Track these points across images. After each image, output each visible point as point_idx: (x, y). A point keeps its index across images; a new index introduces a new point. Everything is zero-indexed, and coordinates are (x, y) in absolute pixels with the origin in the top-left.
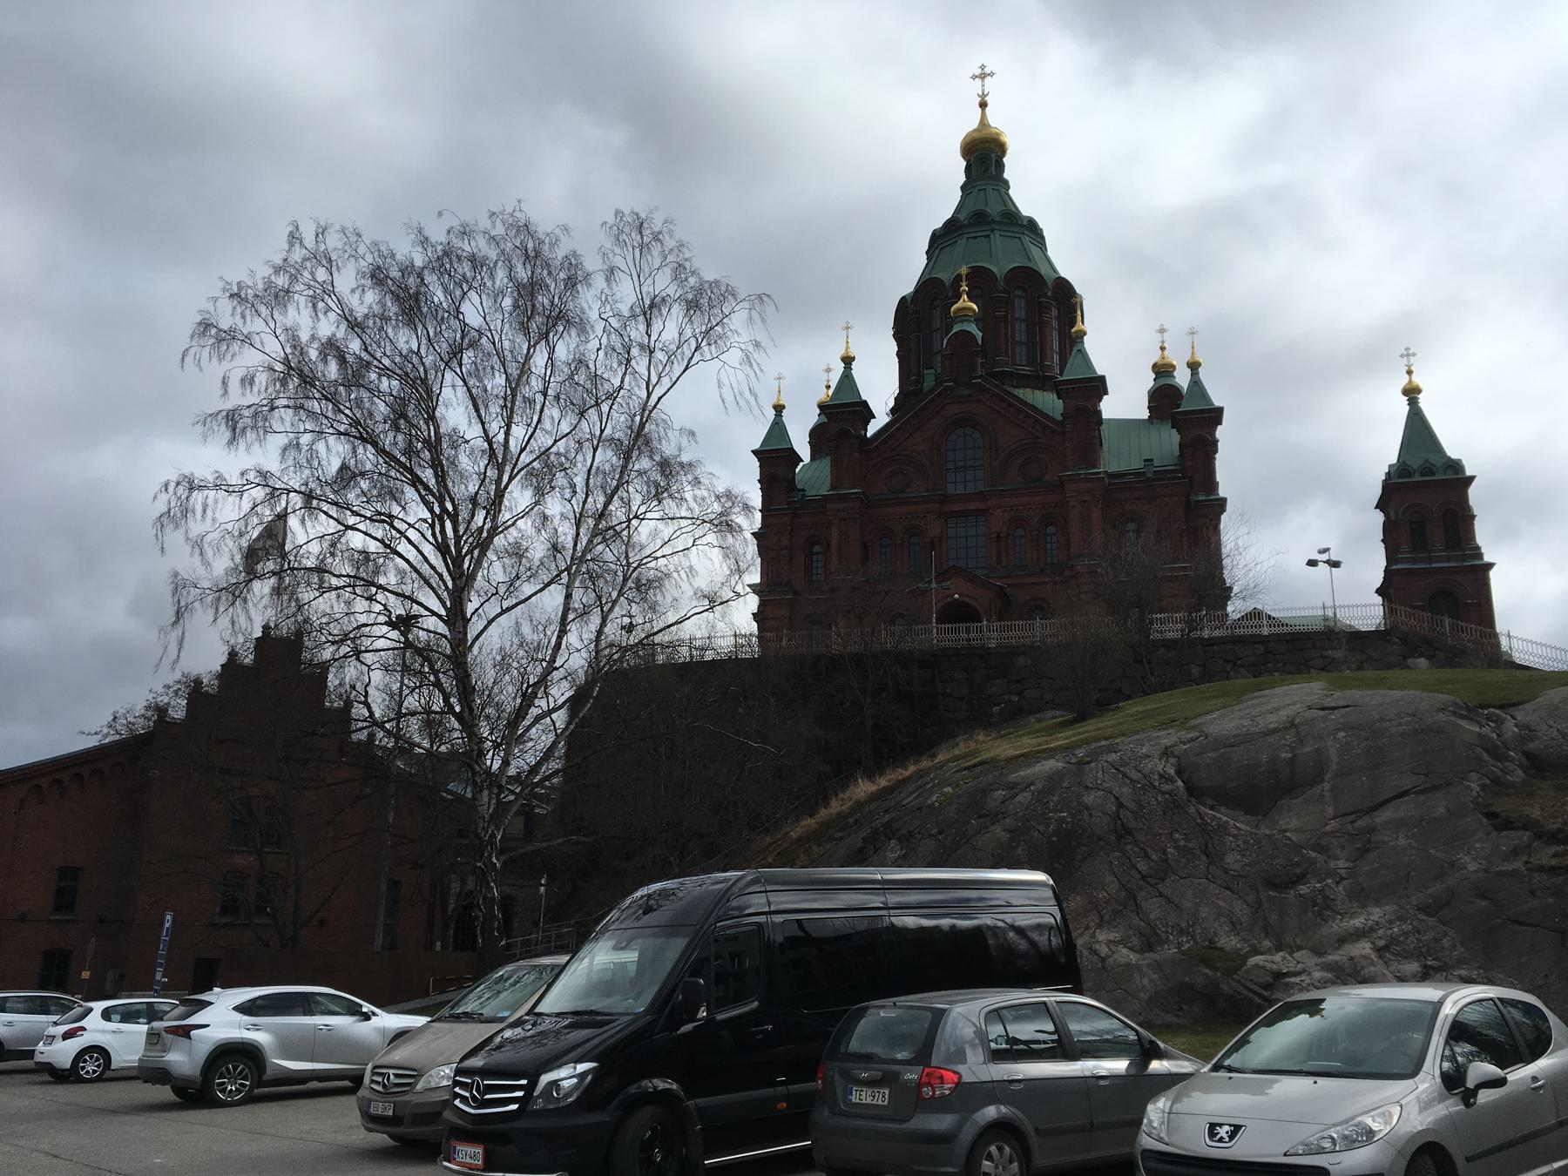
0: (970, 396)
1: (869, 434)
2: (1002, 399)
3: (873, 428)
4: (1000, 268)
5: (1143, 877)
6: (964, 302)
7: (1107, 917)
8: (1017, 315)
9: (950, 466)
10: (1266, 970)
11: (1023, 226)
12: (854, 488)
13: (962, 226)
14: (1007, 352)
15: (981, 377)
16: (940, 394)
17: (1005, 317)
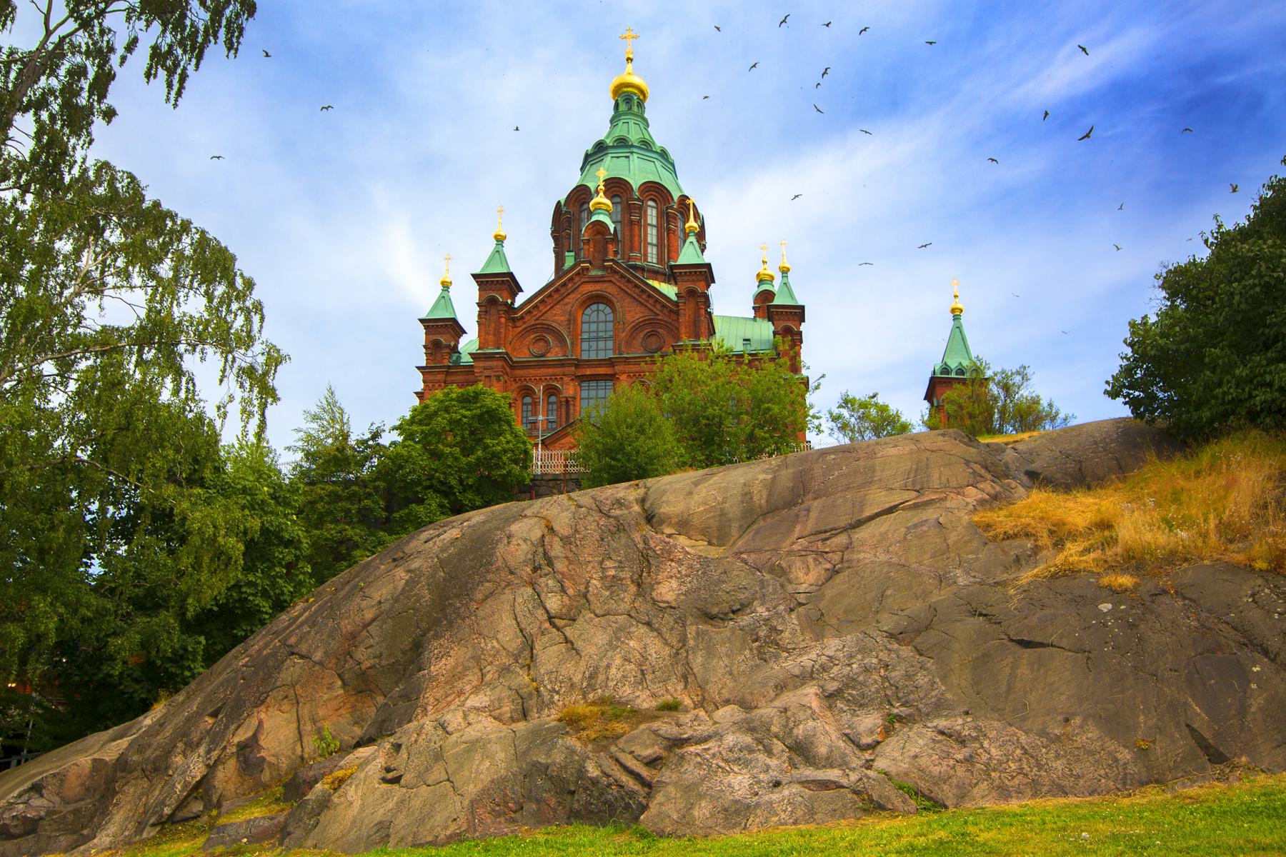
0: (603, 276)
1: (516, 305)
2: (629, 281)
3: (520, 299)
4: (636, 182)
5: (550, 618)
6: (601, 199)
7: (488, 677)
8: (649, 221)
10: (659, 735)
11: (656, 152)
12: (498, 348)
13: (608, 147)
14: (640, 252)
15: (612, 260)
16: (578, 274)
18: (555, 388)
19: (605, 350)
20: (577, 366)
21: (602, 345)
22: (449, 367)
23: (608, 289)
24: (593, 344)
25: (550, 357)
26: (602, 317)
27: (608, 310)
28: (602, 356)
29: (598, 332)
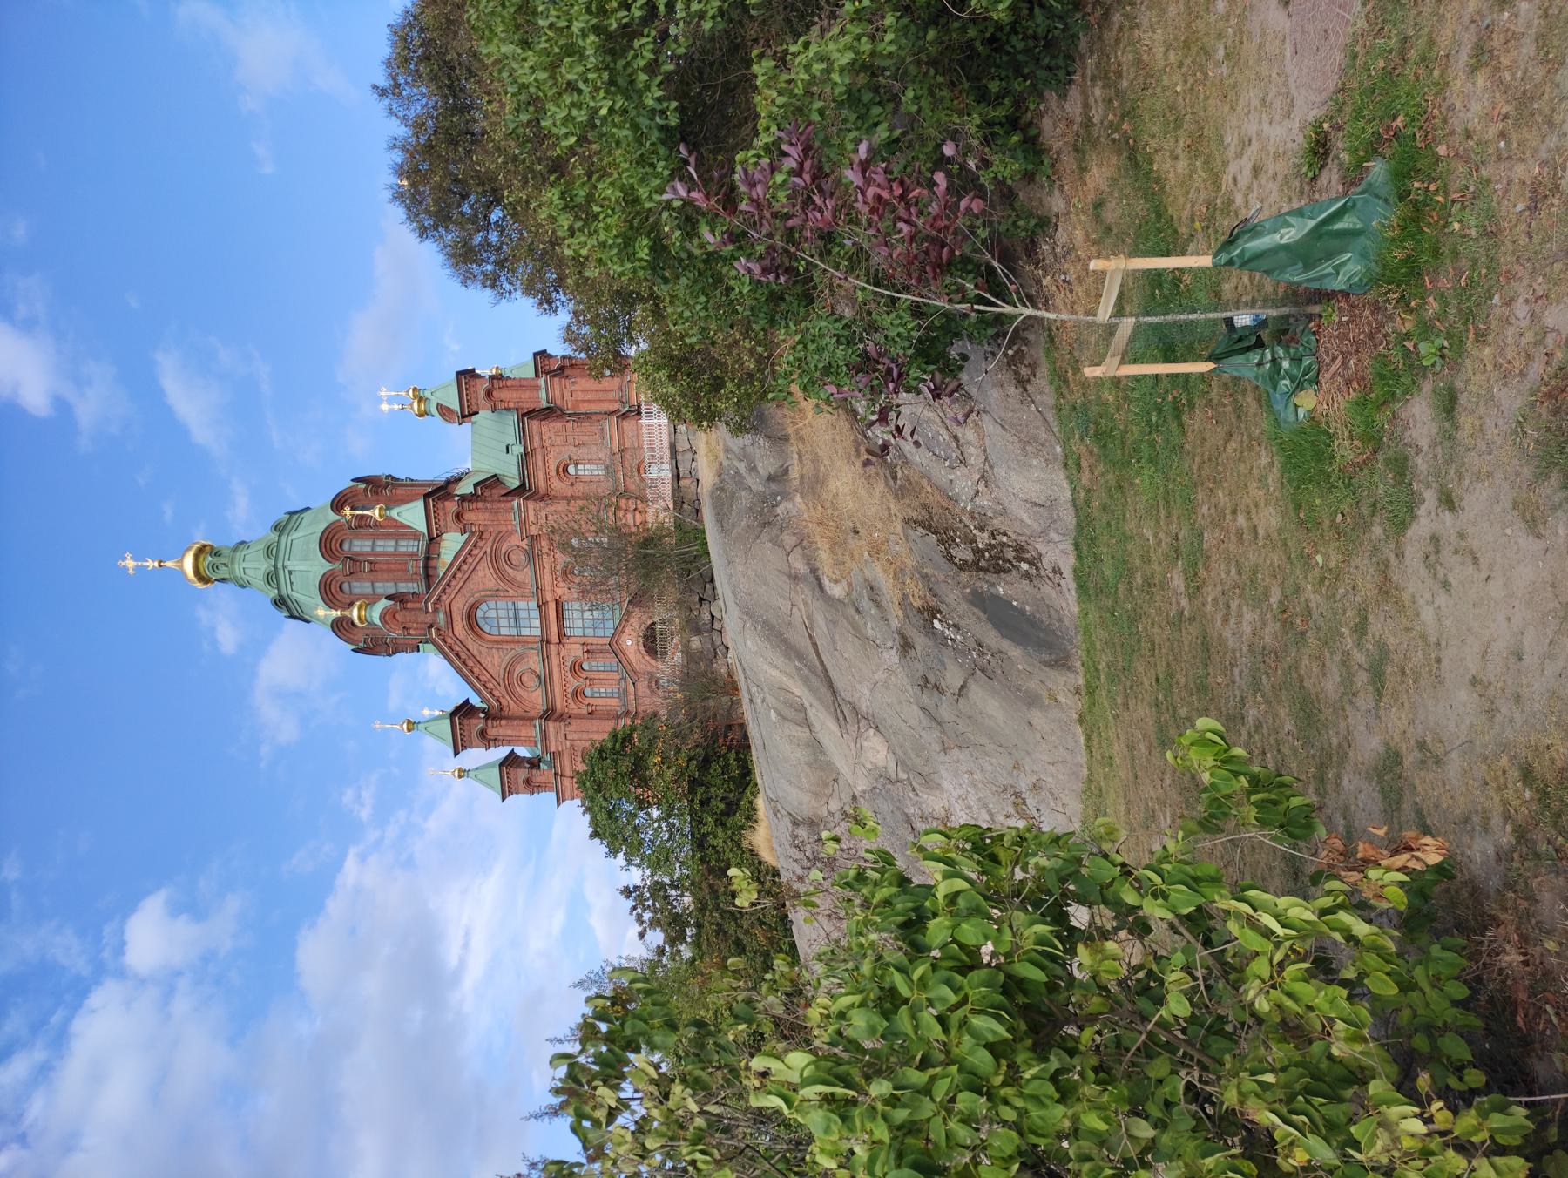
3: (476, 701)
4: (320, 566)
8: (369, 549)
9: (514, 632)
14: (406, 563)
16: (444, 640)
17: (371, 562)
18: (573, 665)
19: (528, 607)
20: (548, 642)
21: (523, 614)
22: (556, 774)
23: (459, 606)
24: (523, 623)
25: (539, 669)
26: (492, 614)
27: (484, 607)
28: (535, 614)
29: (509, 618)
